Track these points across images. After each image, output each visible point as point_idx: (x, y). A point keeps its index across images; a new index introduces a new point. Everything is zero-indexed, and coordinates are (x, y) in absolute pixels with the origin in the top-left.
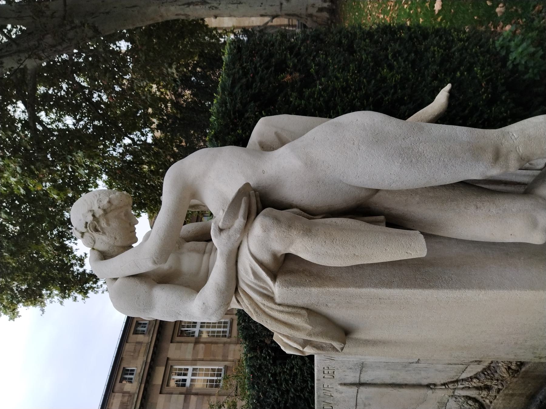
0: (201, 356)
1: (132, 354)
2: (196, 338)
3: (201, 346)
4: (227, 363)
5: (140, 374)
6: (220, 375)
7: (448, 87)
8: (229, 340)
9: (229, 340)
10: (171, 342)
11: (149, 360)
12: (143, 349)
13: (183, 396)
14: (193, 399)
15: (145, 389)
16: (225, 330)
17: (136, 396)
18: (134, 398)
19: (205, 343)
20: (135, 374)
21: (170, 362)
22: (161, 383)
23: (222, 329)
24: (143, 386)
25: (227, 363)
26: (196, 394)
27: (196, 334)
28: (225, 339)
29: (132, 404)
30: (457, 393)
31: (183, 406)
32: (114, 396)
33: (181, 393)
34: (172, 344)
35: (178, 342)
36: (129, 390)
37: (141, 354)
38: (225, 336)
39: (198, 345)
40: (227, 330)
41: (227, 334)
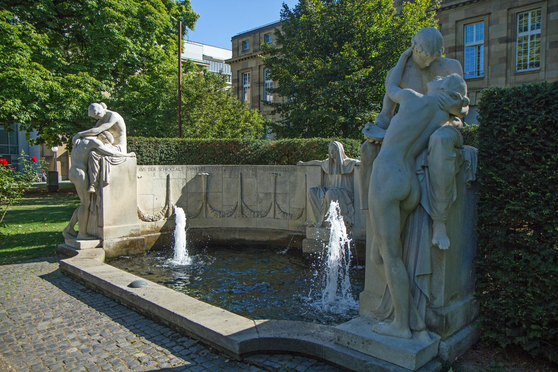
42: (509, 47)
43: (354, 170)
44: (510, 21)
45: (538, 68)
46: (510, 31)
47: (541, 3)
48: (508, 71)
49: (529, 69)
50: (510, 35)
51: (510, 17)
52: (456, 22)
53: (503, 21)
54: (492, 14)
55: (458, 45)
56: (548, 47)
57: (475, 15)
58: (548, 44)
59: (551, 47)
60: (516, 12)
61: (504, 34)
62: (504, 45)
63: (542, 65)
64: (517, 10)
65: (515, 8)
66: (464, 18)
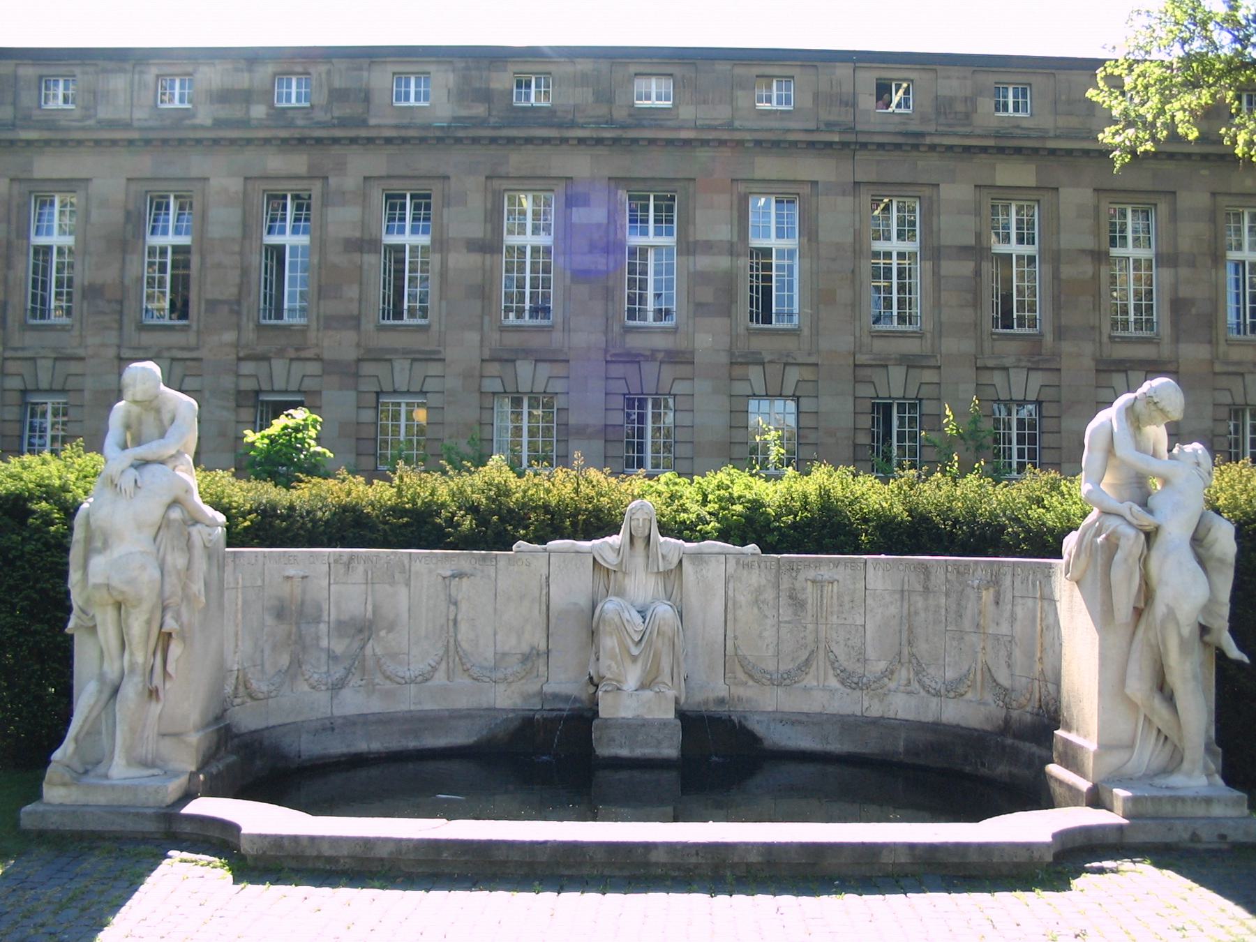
0: (1067, 271)
1: (1063, 98)
2: (1107, 253)
3: (1086, 268)
4: (1049, 338)
5: (1018, 127)
6: (1021, 325)
7: (1246, 659)
8: (1105, 339)
9: (1105, 339)
10: (1095, 190)
11: (1051, 144)
12: (1074, 122)
13: (970, 240)
14: (966, 268)
15: (984, 149)
16: (1132, 326)
17: (968, 129)
18: (963, 125)
19: (1096, 277)
20: (1017, 115)
21: (1046, 197)
22: (998, 184)
23: (1132, 317)
24: (991, 142)
25: (1049, 338)
26: (978, 273)
27: (1116, 252)
28: (1106, 328)
29: (950, 126)
30: (1036, 683)
31: (949, 247)
32: (965, 78)
33: (978, 236)
34: (1089, 192)
35: (1097, 209)
36: (979, 111)
37: (1063, 122)
38: (1114, 324)
39: (1089, 259)
40: (1132, 332)
41: (1120, 333)
42: (488, 263)
43: (681, 561)
44: (489, 206)
45: (545, 322)
46: (489, 226)
47: (555, 182)
48: (487, 319)
49: (527, 320)
50: (489, 236)
51: (489, 196)
52: (366, 178)
53: (477, 203)
54: (453, 180)
55: (367, 237)
56: (568, 281)
57: (410, 173)
58: (568, 274)
59: (572, 280)
60: (504, 187)
61: (477, 231)
62: (475, 259)
63: (556, 316)
64: (505, 184)
65: (500, 177)
66: (383, 173)
